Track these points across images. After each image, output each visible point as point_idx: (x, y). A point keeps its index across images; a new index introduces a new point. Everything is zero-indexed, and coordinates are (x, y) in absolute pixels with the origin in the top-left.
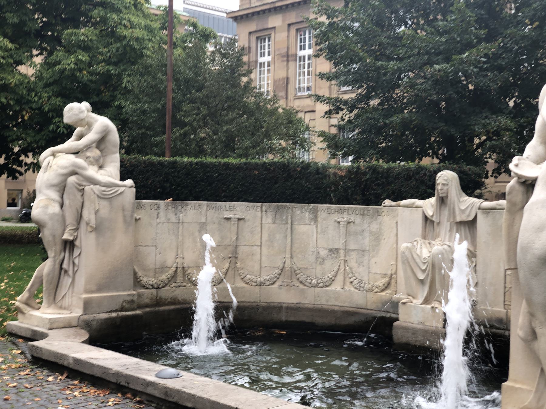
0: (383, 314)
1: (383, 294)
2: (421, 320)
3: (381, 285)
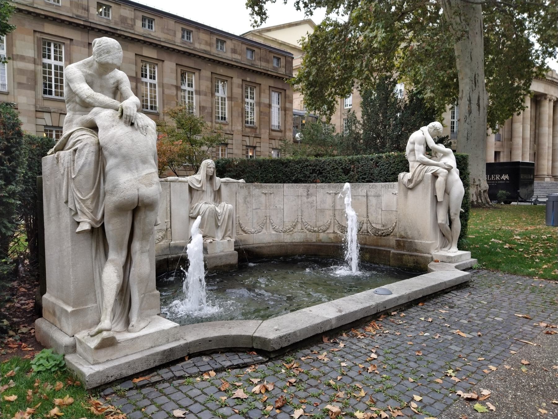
0: (166, 257)
1: (162, 243)
2: (222, 249)
3: (160, 237)
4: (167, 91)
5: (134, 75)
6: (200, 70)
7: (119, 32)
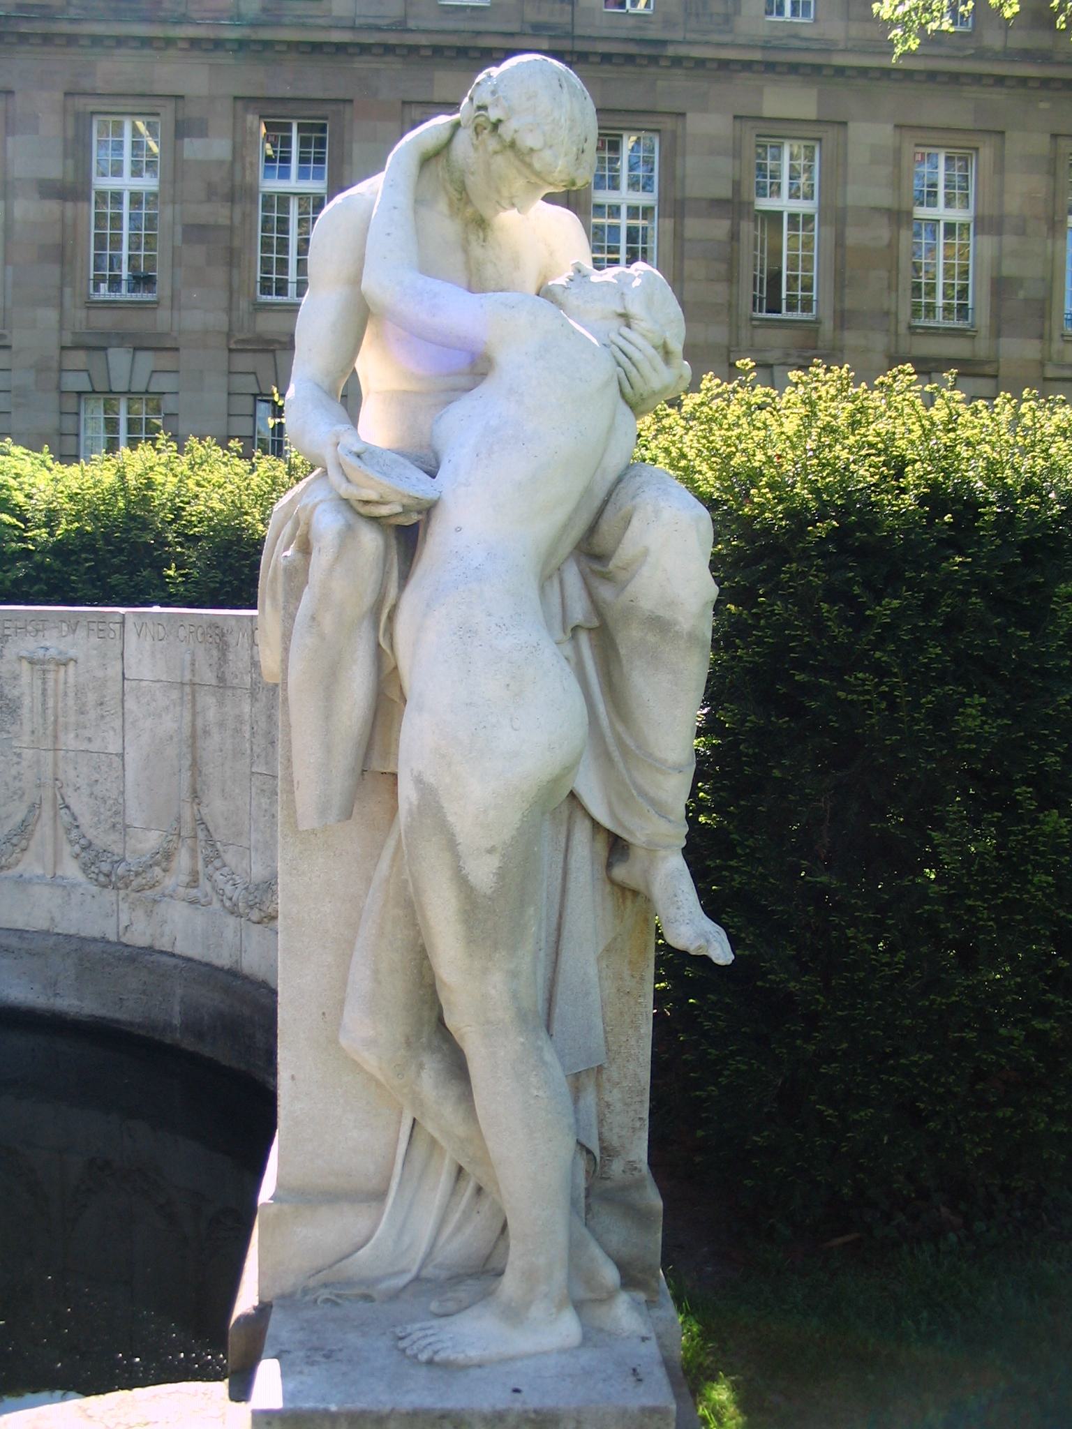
4: (853, 236)
5: (725, 191)
6: (1002, 133)
7: (671, 51)
